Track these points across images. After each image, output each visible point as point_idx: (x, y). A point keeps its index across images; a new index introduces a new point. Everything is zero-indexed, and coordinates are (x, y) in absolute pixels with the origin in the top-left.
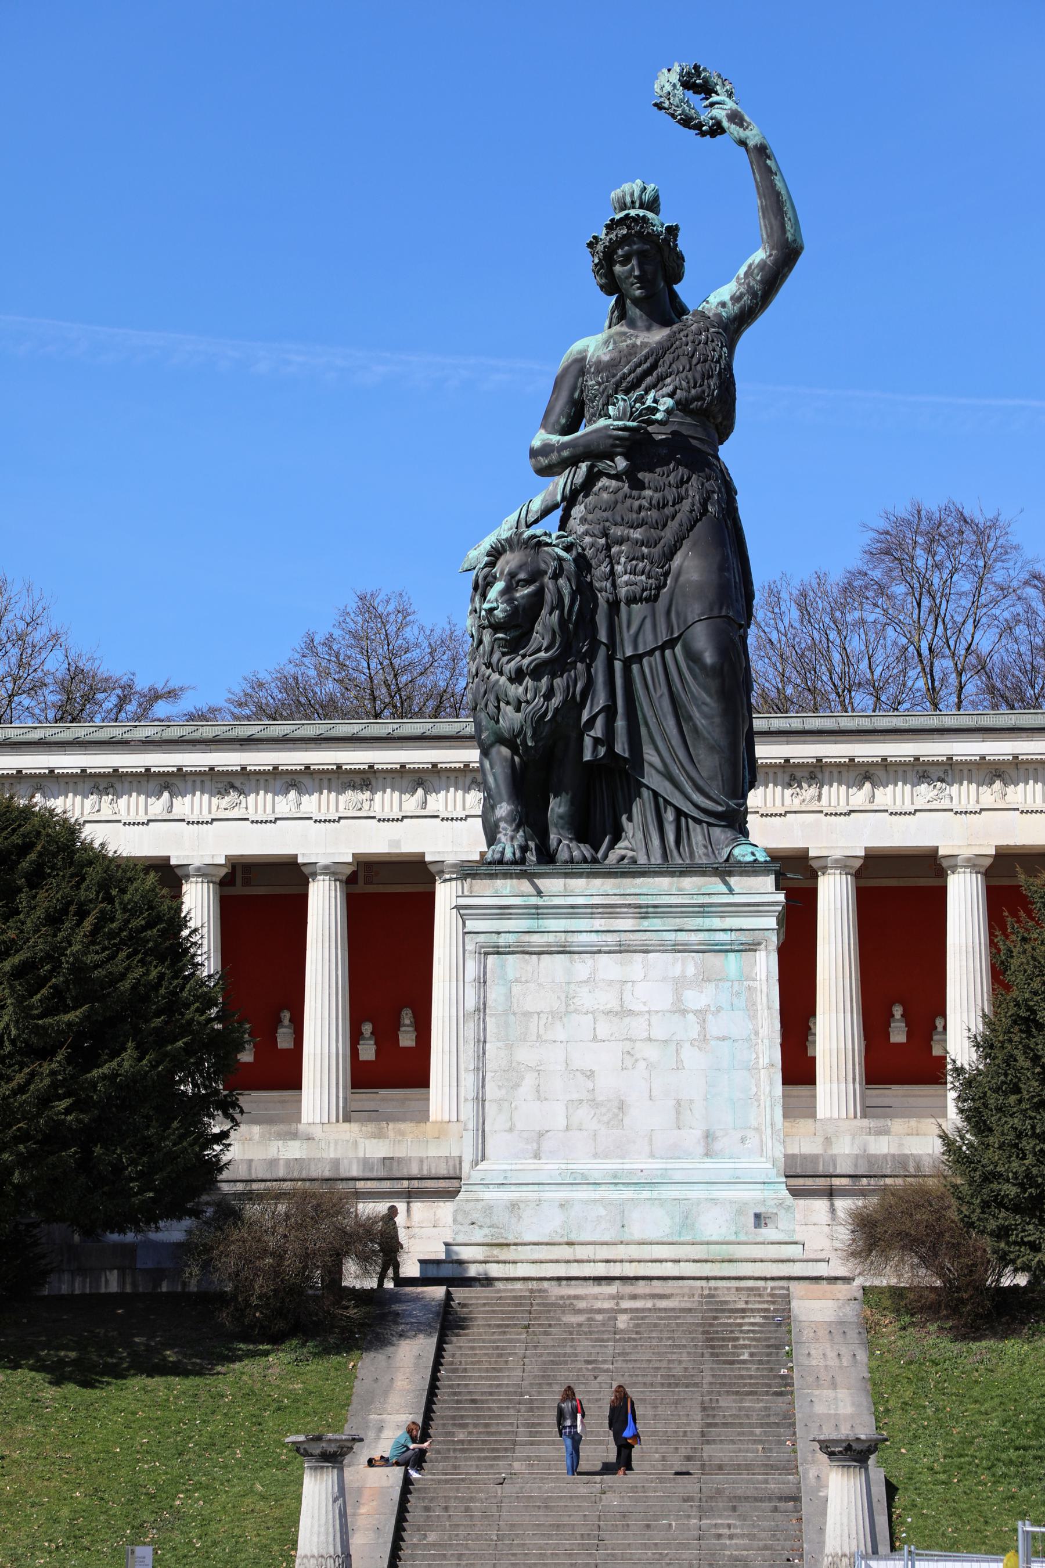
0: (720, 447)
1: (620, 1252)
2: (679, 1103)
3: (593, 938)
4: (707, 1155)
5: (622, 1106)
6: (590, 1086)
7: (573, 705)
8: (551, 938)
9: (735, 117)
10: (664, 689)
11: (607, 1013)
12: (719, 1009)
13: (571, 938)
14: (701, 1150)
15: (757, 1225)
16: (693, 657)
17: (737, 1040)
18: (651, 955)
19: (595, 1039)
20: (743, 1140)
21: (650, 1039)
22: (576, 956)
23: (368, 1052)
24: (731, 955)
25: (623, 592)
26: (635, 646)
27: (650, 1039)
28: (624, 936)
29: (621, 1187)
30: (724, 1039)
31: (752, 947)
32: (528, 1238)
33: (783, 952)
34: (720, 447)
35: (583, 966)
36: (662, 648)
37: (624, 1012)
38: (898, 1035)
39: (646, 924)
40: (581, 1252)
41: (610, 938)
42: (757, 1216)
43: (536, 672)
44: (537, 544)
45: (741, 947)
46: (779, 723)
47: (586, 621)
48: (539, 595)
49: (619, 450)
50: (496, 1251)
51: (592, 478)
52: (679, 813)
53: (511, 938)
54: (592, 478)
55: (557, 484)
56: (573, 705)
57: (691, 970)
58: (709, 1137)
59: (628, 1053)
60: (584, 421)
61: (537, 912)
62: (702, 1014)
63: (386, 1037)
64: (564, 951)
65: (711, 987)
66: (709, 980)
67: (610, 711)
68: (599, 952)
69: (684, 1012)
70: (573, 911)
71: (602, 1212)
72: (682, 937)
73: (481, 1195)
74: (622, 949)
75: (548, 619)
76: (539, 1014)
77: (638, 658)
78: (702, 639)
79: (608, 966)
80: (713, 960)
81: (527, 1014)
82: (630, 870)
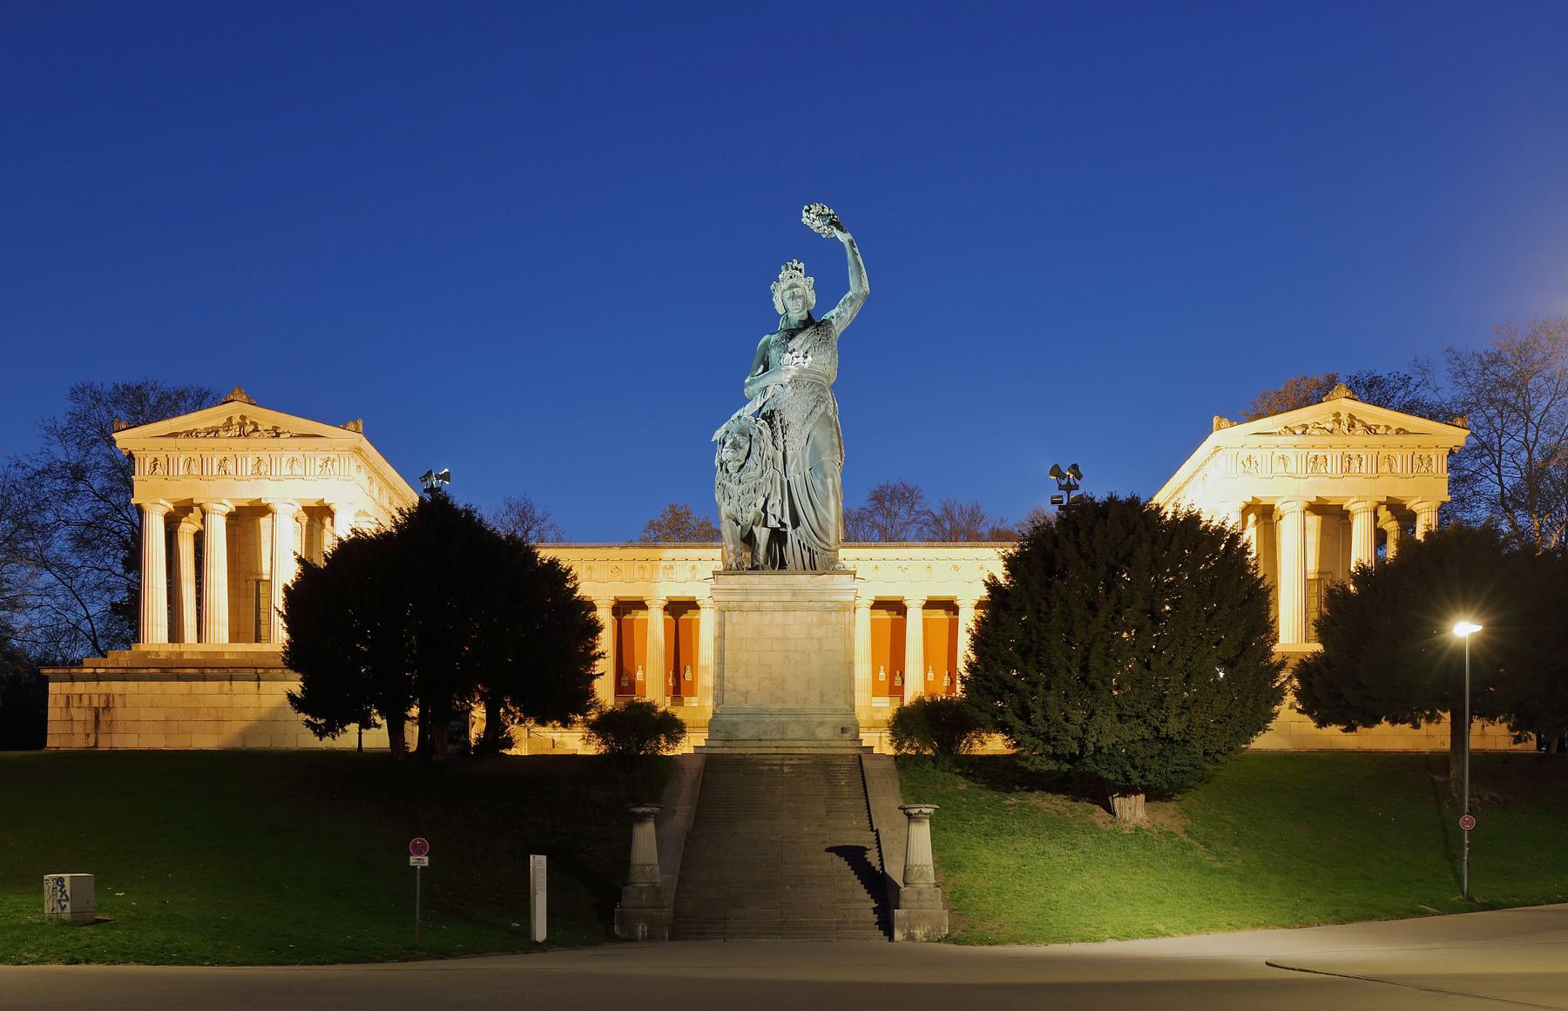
1: (783, 743)
2: (809, 680)
6: (769, 671)
8: (753, 604)
11: (777, 639)
12: (827, 637)
14: (819, 699)
15: (843, 733)
18: (798, 613)
19: (772, 651)
20: (837, 696)
21: (796, 651)
27: (796, 651)
28: (786, 604)
32: (741, 737)
39: (795, 599)
40: (763, 743)
41: (779, 604)
50: (727, 743)
53: (735, 604)
57: (815, 620)
66: (822, 625)
73: (720, 719)
74: (785, 610)
81: (742, 639)
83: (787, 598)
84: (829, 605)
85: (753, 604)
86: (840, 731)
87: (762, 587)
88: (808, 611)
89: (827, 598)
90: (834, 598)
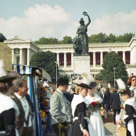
0: (87, 33)
7: (79, 47)
9: (87, 15)
16: (85, 44)
23: (68, 63)
31: (88, 60)
33: (90, 60)
34: (87, 33)
38: (98, 62)
43: (77, 45)
44: (77, 38)
46: (91, 46)
47: (79, 42)
48: (77, 41)
51: (79, 35)
54: (79, 35)
56: (79, 47)
60: (75, 53)
61: (77, 58)
63: (69, 62)
74: (82, 60)
75: (77, 42)
78: (85, 43)
82: (82, 55)
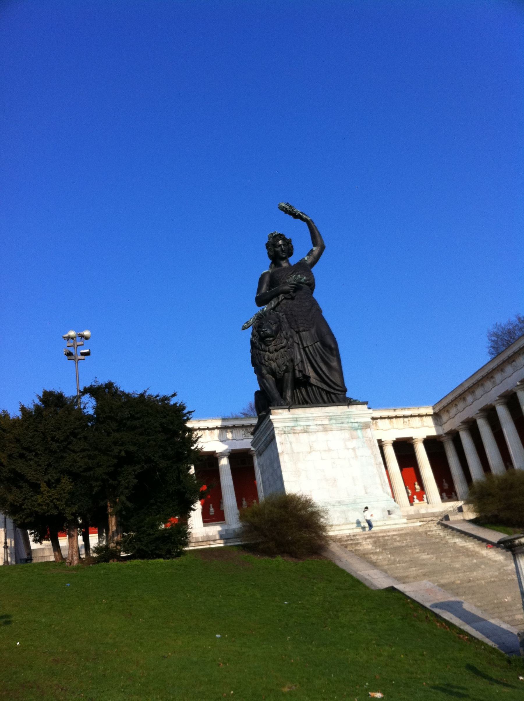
3: (315, 427)
4: (366, 494)
5: (335, 480)
10: (318, 356)
11: (325, 451)
12: (359, 447)
13: (308, 428)
17: (367, 457)
18: (333, 431)
19: (322, 459)
21: (339, 458)
22: (310, 433)
24: (359, 431)
25: (301, 329)
26: (307, 344)
27: (339, 458)
29: (341, 506)
30: (362, 456)
35: (313, 437)
36: (314, 344)
37: (329, 450)
39: (331, 422)
41: (321, 427)
42: (389, 511)
45: (362, 428)
49: (292, 291)
52: (328, 392)
53: (289, 429)
55: (271, 303)
58: (365, 488)
59: (333, 463)
62: (354, 449)
64: (306, 432)
65: (355, 441)
66: (353, 439)
67: (302, 361)
68: (318, 431)
69: (348, 449)
70: (308, 419)
71: (338, 514)
72: (343, 425)
74: (326, 430)
76: (302, 452)
77: (308, 347)
79: (321, 436)
80: (355, 433)
81: (298, 453)
83: (326, 422)
84: (356, 425)
85: (302, 428)
86: (387, 513)
87: (307, 415)
88: (341, 430)
89: (353, 421)
90: (356, 420)
